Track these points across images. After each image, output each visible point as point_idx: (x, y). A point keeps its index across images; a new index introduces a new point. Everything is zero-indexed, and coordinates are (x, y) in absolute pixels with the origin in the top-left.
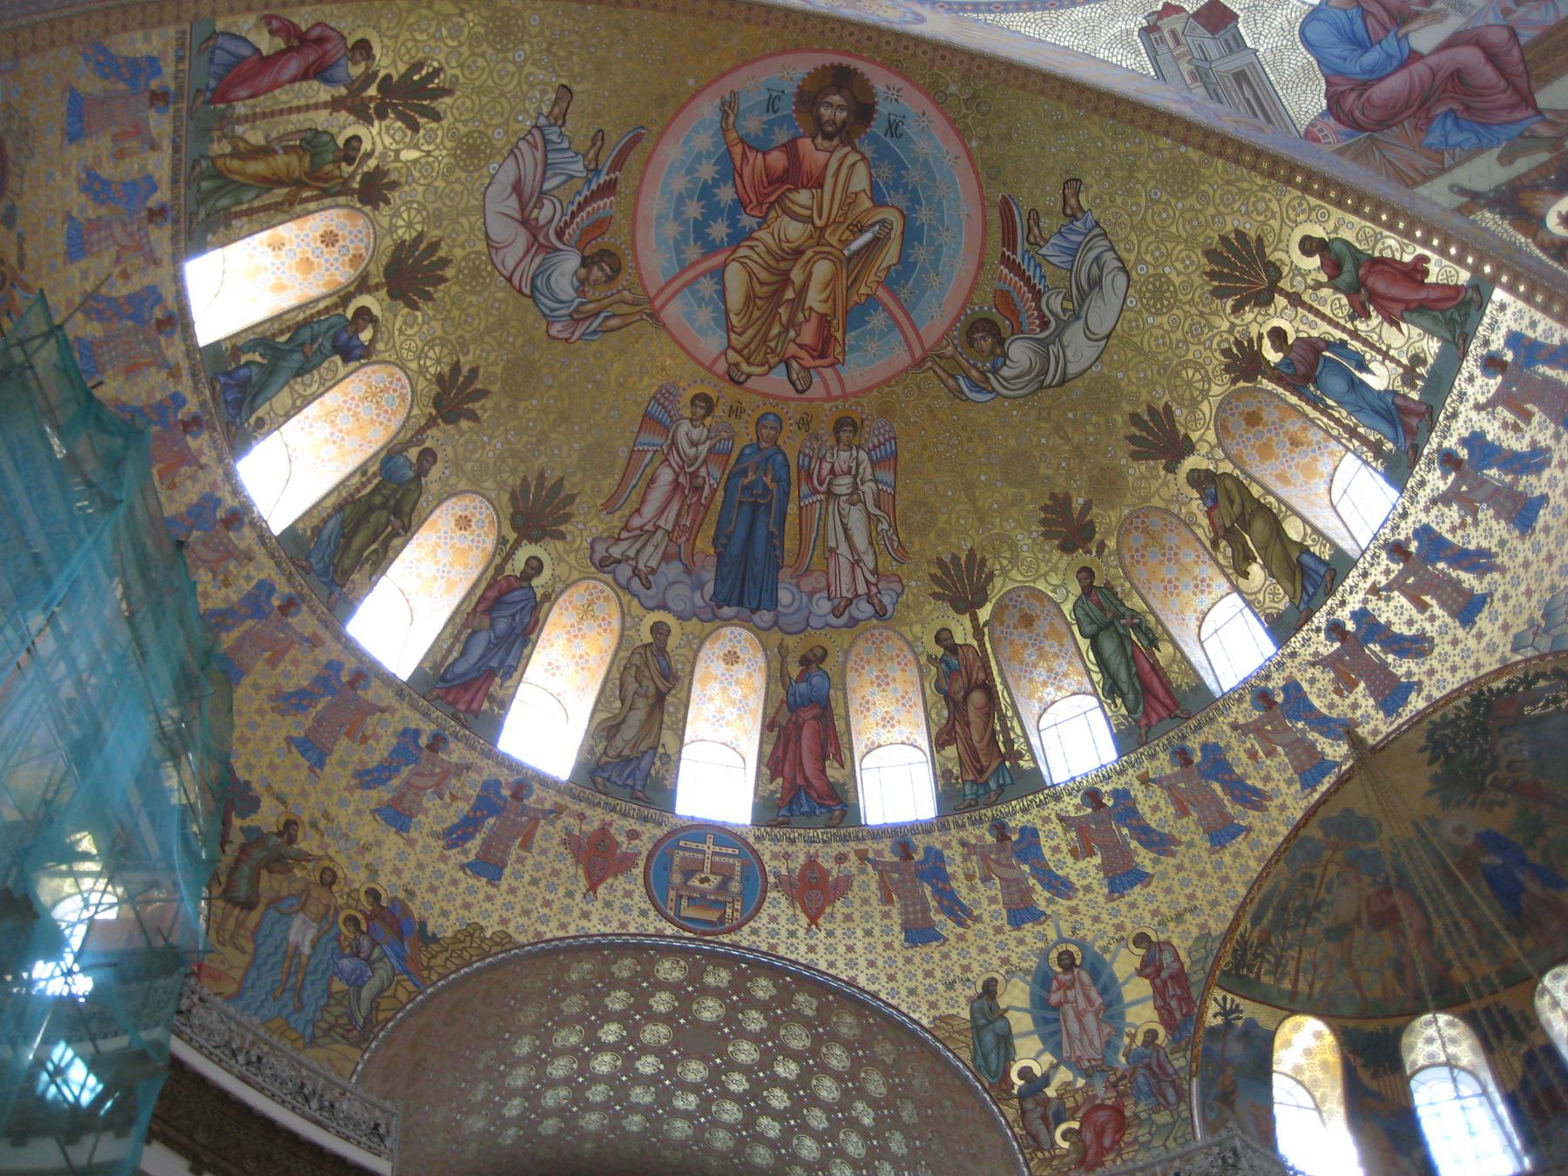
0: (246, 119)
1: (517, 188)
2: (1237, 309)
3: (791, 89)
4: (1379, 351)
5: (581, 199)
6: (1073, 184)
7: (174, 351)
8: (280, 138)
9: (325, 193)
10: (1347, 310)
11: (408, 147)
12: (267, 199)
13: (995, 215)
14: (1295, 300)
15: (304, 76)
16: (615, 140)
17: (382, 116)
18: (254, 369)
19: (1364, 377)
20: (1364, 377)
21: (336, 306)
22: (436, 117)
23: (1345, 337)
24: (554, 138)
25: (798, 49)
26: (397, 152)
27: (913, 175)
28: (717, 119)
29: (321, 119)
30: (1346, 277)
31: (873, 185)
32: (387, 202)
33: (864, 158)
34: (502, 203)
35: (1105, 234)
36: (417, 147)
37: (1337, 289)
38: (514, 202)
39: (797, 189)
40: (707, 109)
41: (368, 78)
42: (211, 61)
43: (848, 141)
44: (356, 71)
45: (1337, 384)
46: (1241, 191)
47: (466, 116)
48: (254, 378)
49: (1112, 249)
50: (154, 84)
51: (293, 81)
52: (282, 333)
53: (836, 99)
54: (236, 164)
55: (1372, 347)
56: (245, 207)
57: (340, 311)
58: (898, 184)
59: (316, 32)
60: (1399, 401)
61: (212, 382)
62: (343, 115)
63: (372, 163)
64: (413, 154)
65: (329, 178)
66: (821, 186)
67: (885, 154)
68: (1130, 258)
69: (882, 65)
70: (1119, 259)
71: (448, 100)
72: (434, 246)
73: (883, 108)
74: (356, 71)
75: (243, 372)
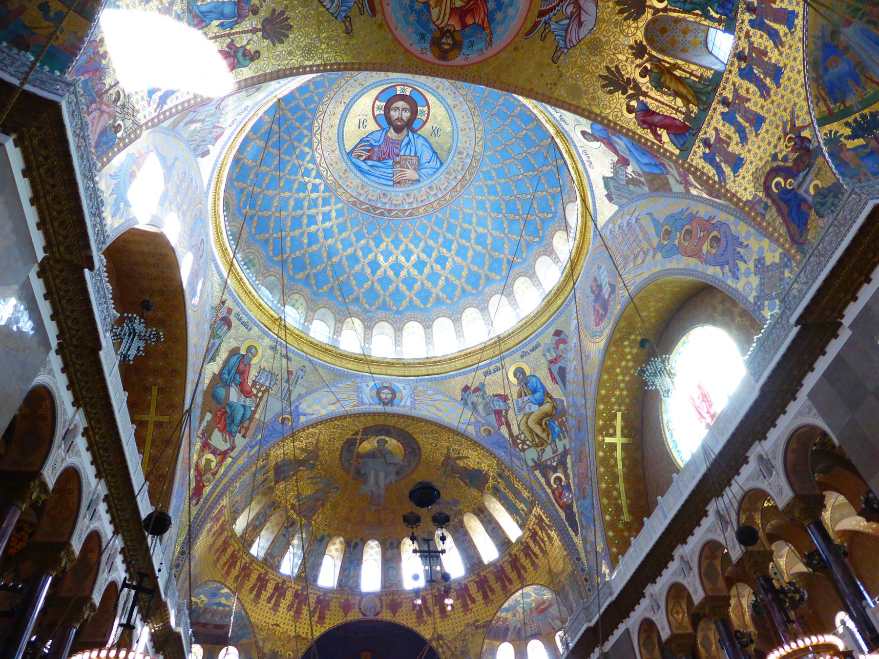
0: (680, 112)
1: (580, 24)
2: (274, 10)
3: (464, 51)
4: (219, 37)
5: (554, 12)
6: (348, 32)
7: (744, 44)
8: (669, 95)
9: (660, 60)
10: (235, 43)
11: (622, 61)
12: (684, 75)
13: (378, 8)
14: (254, 31)
15: (654, 113)
16: (537, 34)
17: (628, 79)
18: (715, 8)
19: (219, 22)
20: (219, 22)
21: (670, 10)
22: (607, 68)
23: (232, 31)
24: (561, 42)
25: (462, 67)
26: (626, 61)
27: (413, 18)
28: (493, 40)
29: (653, 93)
30: (240, 54)
31: (429, 12)
32: (636, 41)
33: (434, 23)
34: (588, 19)
35: (332, 14)
36: (618, 60)
37: (242, 47)
38: (583, 18)
39: (461, 7)
40: (498, 45)
41: (631, 97)
42: (685, 142)
43: (440, 29)
44: (634, 103)
45: (228, 10)
46: (286, 59)
47: (596, 64)
48: (717, 5)
49: (328, 10)
50: (707, 151)
51: (658, 114)
52: (697, 15)
53: (446, 47)
54: (690, 97)
55: (221, 36)
56: (692, 78)
57: (669, 7)
58: (419, 13)
59: (645, 126)
60: (204, 24)
61: (735, 18)
62: (644, 89)
63: (638, 61)
64: (620, 57)
65: (657, 66)
66: (451, 9)
67: (424, 25)
68: (322, 9)
69: (429, 62)
70: (324, 6)
71: (601, 73)
72: (621, 12)
73: (427, 45)
74: (634, 103)
75: (721, 12)
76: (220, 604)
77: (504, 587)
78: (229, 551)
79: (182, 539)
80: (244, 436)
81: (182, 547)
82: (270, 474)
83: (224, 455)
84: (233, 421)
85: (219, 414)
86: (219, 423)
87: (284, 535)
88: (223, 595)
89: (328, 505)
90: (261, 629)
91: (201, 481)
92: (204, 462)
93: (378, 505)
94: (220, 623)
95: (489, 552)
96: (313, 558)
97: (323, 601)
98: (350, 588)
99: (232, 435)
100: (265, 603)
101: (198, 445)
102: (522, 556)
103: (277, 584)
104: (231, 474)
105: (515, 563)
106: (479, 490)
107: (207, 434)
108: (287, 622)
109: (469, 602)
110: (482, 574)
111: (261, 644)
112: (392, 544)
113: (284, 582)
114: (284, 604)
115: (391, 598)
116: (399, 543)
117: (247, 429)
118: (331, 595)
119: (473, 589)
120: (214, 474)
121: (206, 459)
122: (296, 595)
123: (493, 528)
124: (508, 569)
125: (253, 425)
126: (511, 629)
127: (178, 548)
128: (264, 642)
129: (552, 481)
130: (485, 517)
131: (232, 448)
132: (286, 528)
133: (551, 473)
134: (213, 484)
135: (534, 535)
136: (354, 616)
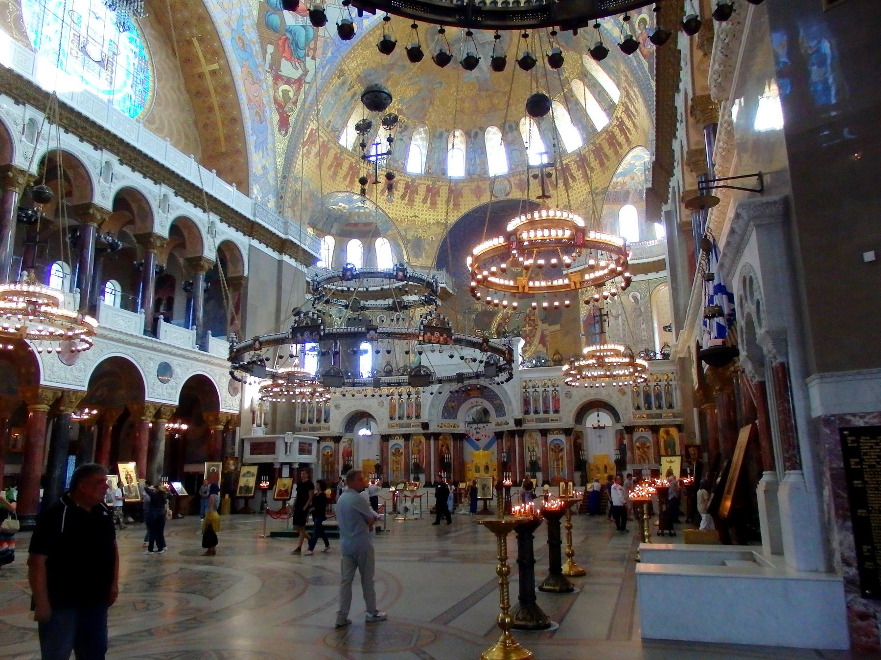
76: (359, 207)
77: (616, 153)
78: (346, 166)
79: (280, 167)
80: (314, 58)
81: (283, 173)
82: (356, 87)
83: (299, 82)
84: (297, 45)
85: (280, 43)
86: (284, 51)
87: (401, 140)
88: (357, 201)
89: (437, 102)
90: (401, 222)
91: (284, 112)
92: (281, 94)
93: (487, 90)
94: (367, 221)
95: (600, 120)
96: (436, 156)
97: (455, 191)
98: (479, 175)
99: (301, 60)
100: (399, 201)
101: (270, 79)
102: (624, 116)
103: (407, 183)
104: (310, 98)
105: (621, 125)
106: (575, 51)
107: (275, 67)
108: (424, 212)
109: (588, 172)
110: (597, 142)
111: (403, 233)
112: (510, 127)
113: (413, 180)
114: (418, 199)
115: (518, 178)
116: (518, 125)
117: (315, 50)
118: (462, 184)
119: (592, 159)
120: (295, 103)
121: (283, 91)
122: (429, 189)
123: (599, 92)
124: (617, 132)
125: (320, 44)
126: (632, 192)
127: (280, 175)
128: (406, 231)
129: (637, 26)
130: (589, 80)
131: (306, 72)
132: (401, 132)
133: (636, 15)
134: (296, 112)
135: (628, 95)
136: (486, 199)
